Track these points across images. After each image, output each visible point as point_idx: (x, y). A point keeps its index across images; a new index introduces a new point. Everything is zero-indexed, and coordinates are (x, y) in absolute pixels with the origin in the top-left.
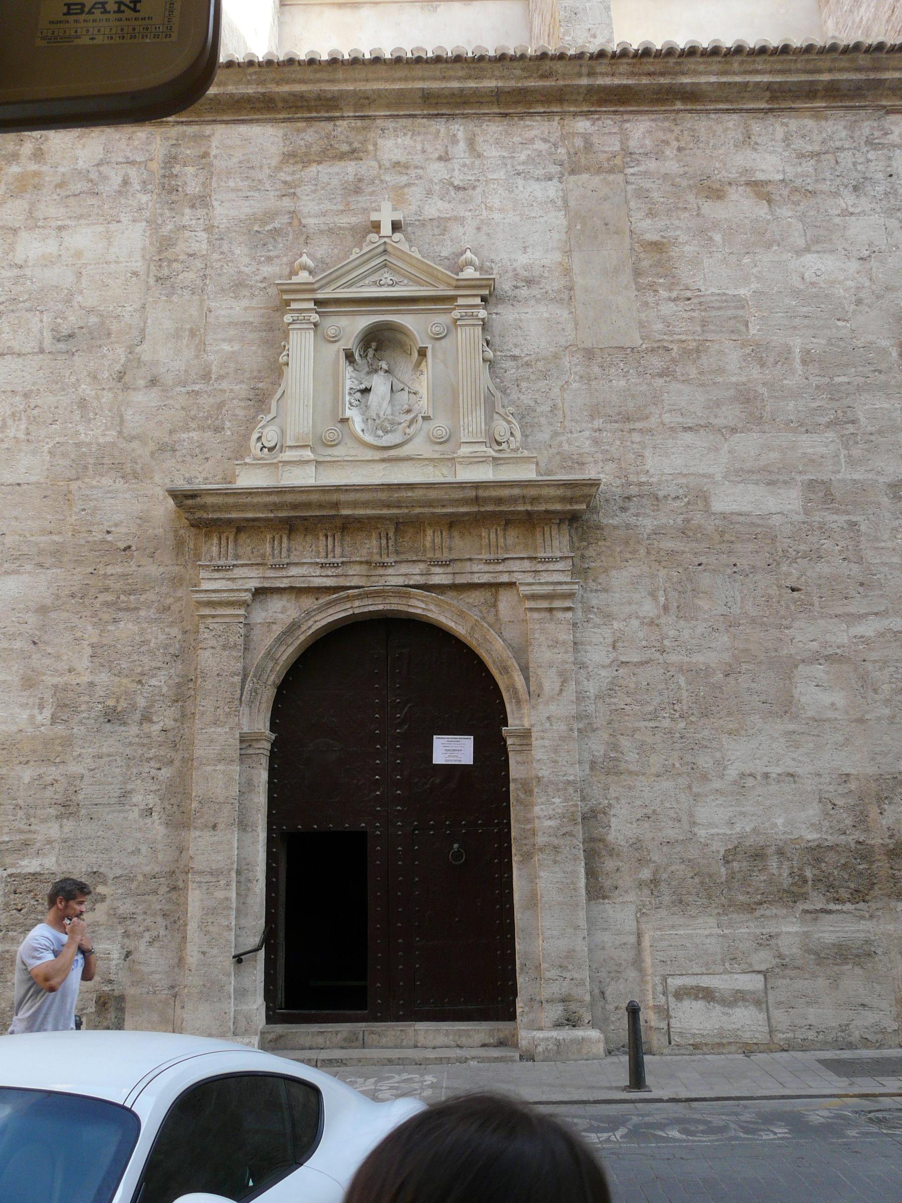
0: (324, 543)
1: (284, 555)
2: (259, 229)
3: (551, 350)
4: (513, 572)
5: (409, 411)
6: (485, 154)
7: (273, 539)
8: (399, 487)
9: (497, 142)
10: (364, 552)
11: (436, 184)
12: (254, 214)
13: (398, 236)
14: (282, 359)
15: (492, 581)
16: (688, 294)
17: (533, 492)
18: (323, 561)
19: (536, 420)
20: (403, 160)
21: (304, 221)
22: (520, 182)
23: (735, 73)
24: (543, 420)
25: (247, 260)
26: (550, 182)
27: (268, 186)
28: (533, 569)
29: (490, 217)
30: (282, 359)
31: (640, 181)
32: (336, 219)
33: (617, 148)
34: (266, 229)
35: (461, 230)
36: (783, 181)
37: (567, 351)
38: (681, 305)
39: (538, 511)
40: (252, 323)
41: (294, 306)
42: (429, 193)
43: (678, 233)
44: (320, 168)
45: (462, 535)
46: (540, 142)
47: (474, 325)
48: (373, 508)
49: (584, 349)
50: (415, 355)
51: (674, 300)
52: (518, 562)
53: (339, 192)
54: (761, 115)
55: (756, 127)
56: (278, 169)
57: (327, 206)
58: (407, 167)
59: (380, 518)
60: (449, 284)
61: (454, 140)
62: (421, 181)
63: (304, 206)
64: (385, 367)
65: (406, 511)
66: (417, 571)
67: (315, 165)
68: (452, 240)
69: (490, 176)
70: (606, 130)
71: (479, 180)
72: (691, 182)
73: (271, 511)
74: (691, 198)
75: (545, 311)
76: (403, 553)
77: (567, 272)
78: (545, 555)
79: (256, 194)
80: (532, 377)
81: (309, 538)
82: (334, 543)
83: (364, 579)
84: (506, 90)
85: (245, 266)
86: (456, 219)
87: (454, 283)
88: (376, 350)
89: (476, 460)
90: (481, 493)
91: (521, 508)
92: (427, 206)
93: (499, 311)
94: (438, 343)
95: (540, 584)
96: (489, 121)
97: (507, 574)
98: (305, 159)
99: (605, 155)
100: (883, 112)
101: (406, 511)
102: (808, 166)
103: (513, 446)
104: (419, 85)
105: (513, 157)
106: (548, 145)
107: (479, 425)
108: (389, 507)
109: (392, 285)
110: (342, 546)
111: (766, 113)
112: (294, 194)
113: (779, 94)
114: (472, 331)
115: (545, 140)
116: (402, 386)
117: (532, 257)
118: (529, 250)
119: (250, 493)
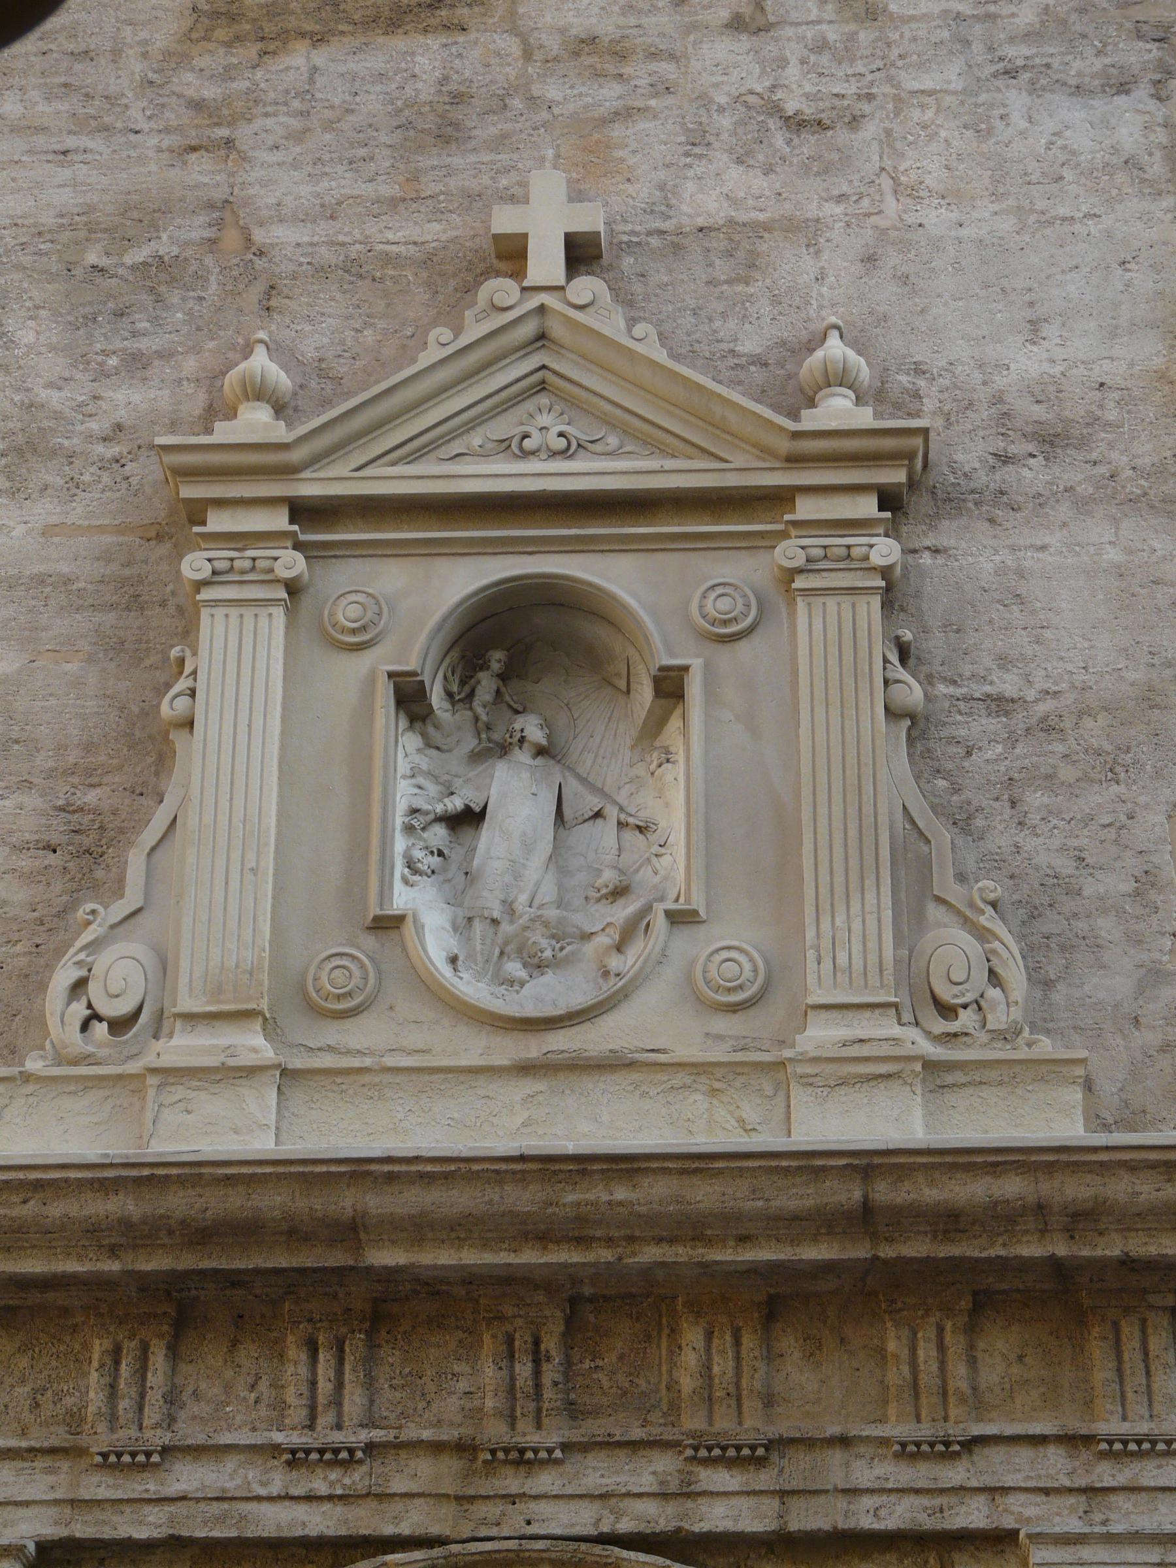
0: (303, 1371)
1: (152, 1415)
2: (104, 262)
3: (1131, 676)
4: (1005, 1490)
5: (619, 892)
7: (116, 1354)
8: (582, 1166)
10: (451, 1406)
11: (721, 110)
12: (89, 209)
13: (586, 287)
14: (171, 707)
15: (929, 1523)
17: (1076, 1190)
18: (296, 1439)
19: (1081, 926)
20: (607, 28)
21: (259, 236)
22: (1016, 100)
24: (1107, 927)
25: (56, 365)
26: (1121, 100)
27: (137, 116)
28: (1082, 1482)
29: (911, 219)
30: (171, 707)
32: (372, 228)
34: (128, 260)
35: (809, 265)
39: (1092, 1261)
40: (68, 581)
41: (218, 522)
42: (698, 141)
44: (320, 57)
45: (813, 1350)
47: (852, 590)
48: (485, 1245)
50: (645, 693)
52: (1024, 1454)
53: (384, 139)
56: (176, 59)
57: (342, 184)
58: (620, 52)
59: (510, 1281)
60: (766, 451)
62: (670, 100)
63: (264, 183)
64: (536, 734)
65: (606, 1255)
66: (646, 1482)
67: (301, 46)
68: (776, 300)
69: (911, 82)
71: (870, 97)
73: (113, 1251)
75: (1105, 539)
76: (595, 1412)
78: (1124, 1428)
79: (95, 143)
80: (1067, 773)
81: (248, 1354)
82: (340, 1372)
83: (448, 1510)
85: (49, 385)
87: (785, 446)
88: (503, 677)
89: (862, 1069)
90: (883, 1192)
91: (1031, 1249)
92: (690, 186)
93: (944, 541)
94: (725, 657)
95: (1110, 1539)
97: (980, 1501)
98: (269, 28)
101: (606, 1255)
103: (998, 1019)
105: (991, 17)
107: (872, 945)
108: (544, 1238)
109: (564, 453)
110: (370, 1383)
112: (229, 143)
114: (847, 615)
116: (595, 803)
117: (1059, 353)
118: (1050, 331)
119: (38, 1185)
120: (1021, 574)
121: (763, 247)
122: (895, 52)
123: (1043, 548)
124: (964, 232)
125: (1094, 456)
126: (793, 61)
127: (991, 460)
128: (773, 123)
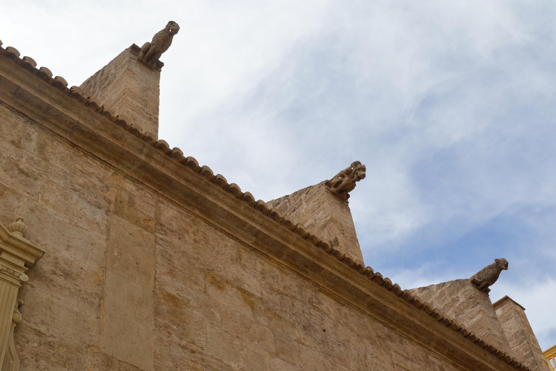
6: (51, 161)
9: (62, 159)
16: (194, 348)
22: (75, 196)
23: (239, 212)
26: (98, 210)
29: (44, 207)
31: (166, 247)
33: (152, 215)
35: (16, 203)
36: (261, 299)
37: (89, 349)
38: (188, 354)
43: (190, 297)
46: (96, 179)
47: (12, 283)
49: (104, 354)
51: (183, 347)
54: (248, 250)
55: (245, 255)
61: (28, 138)
68: (5, 206)
70: (146, 200)
71: (41, 176)
72: (202, 267)
74: (201, 277)
77: (101, 283)
80: (53, 359)
84: (84, 129)
86: (14, 192)
87: (5, 237)
93: (35, 285)
96: (60, 142)
99: (142, 215)
100: (317, 289)
102: (276, 298)
104: (18, 83)
106: (101, 184)
111: (251, 250)
113: (260, 243)
115: (101, 181)
120: (52, 302)
121: (6, 192)
122: (49, 170)
123: (59, 299)
124: (56, 217)
125: (77, 283)
126: (25, 158)
127: (51, 272)
128: (15, 168)
